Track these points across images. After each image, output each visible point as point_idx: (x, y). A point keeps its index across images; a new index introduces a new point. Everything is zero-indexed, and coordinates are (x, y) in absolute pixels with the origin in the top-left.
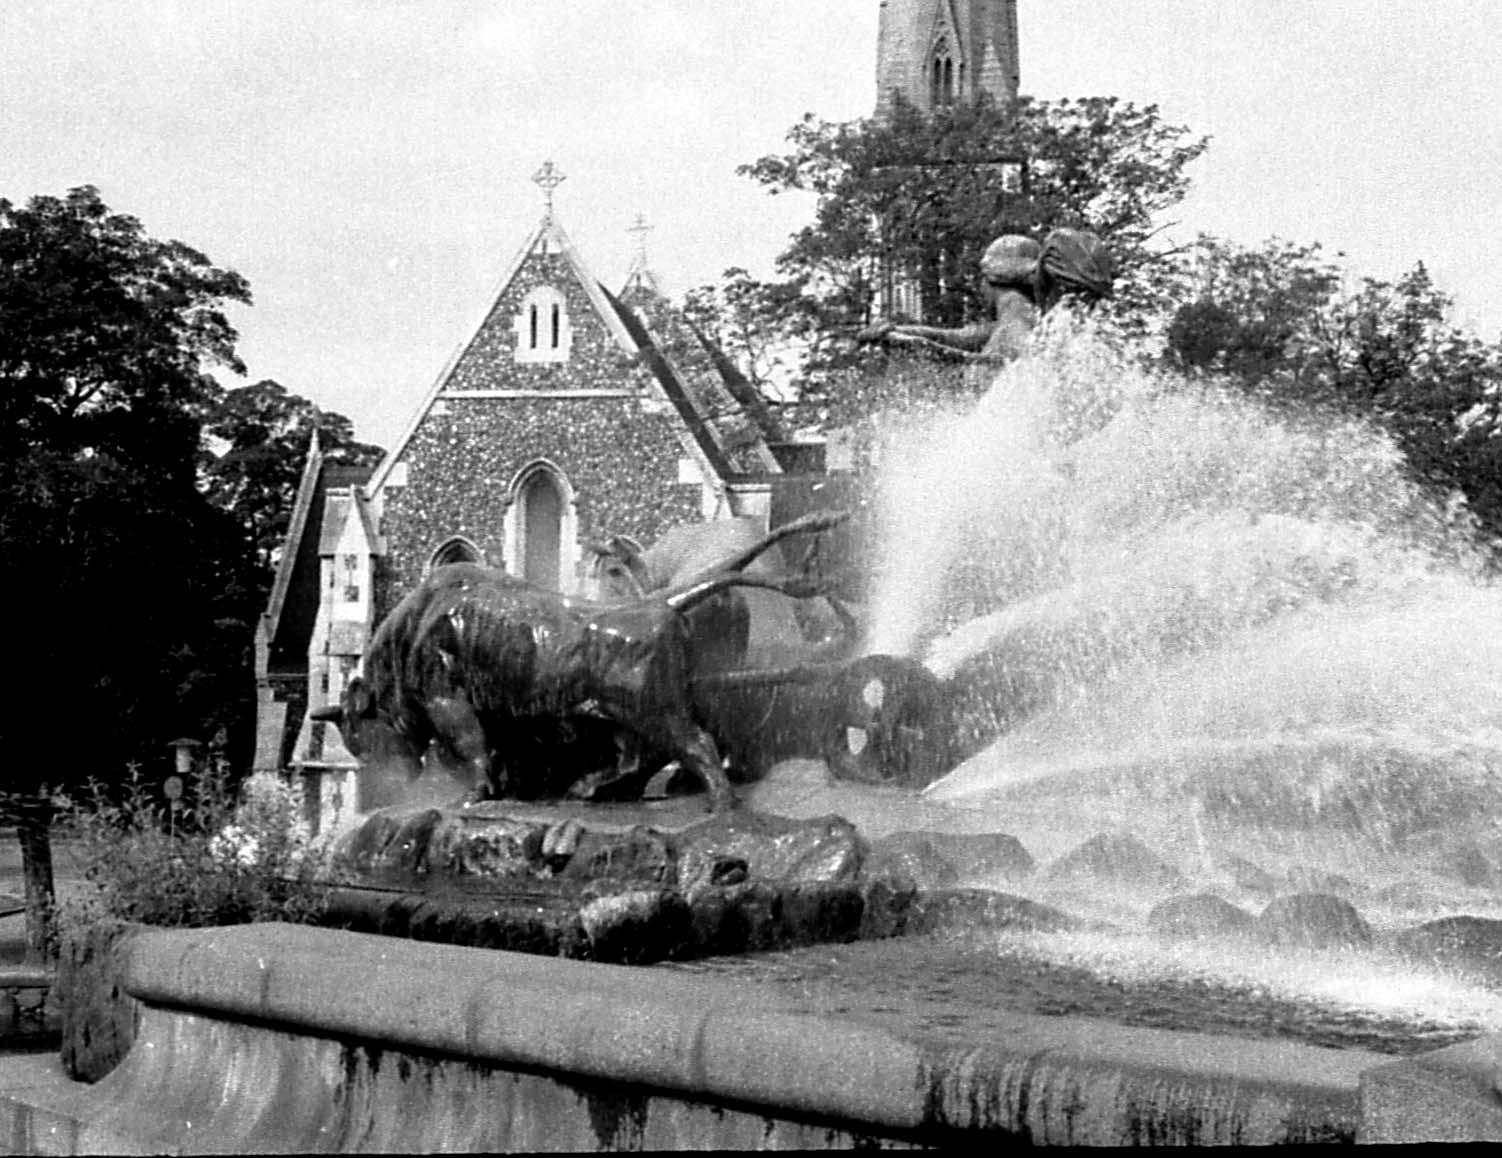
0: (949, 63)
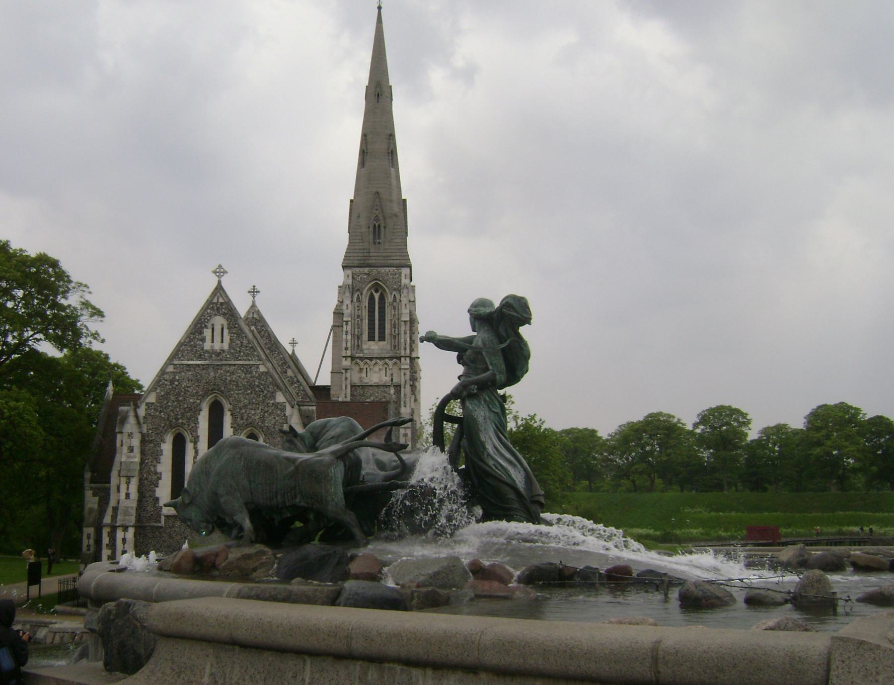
0: (379, 226)
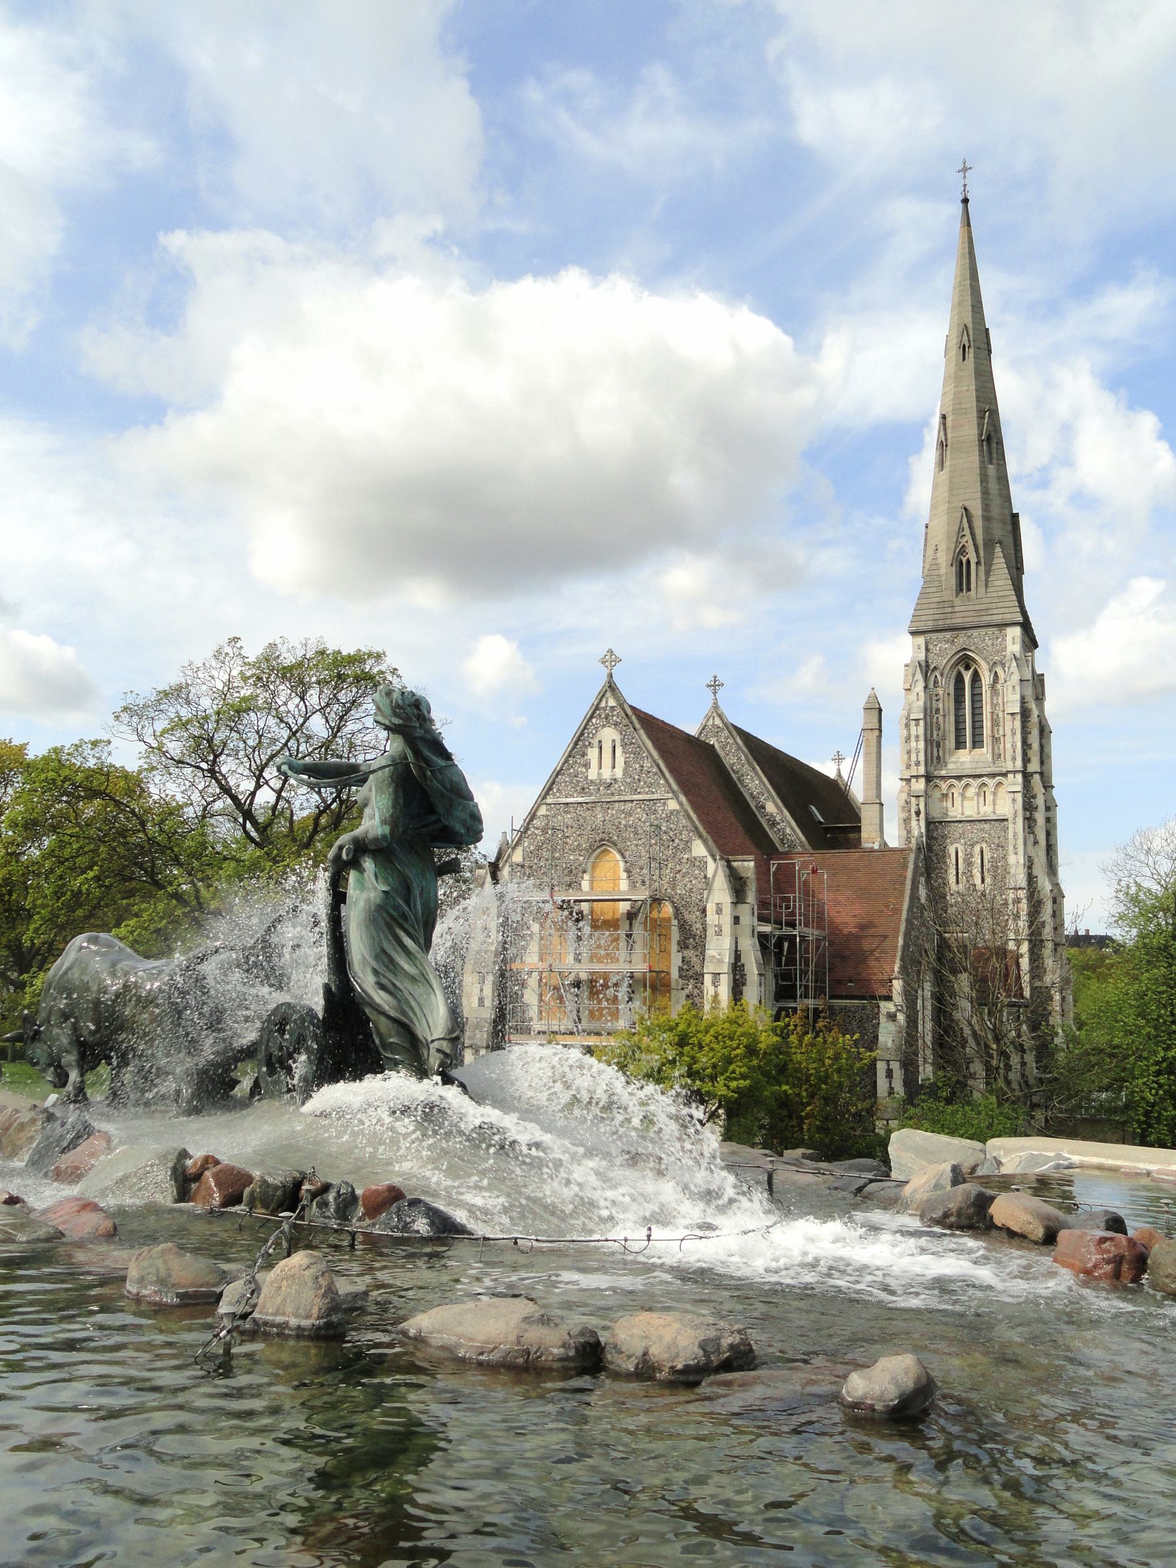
0: (968, 562)
